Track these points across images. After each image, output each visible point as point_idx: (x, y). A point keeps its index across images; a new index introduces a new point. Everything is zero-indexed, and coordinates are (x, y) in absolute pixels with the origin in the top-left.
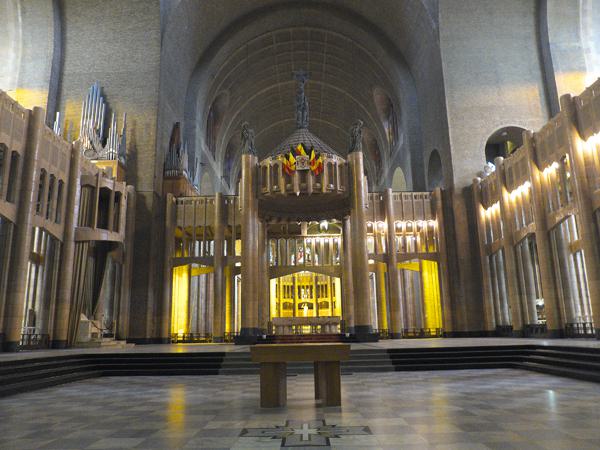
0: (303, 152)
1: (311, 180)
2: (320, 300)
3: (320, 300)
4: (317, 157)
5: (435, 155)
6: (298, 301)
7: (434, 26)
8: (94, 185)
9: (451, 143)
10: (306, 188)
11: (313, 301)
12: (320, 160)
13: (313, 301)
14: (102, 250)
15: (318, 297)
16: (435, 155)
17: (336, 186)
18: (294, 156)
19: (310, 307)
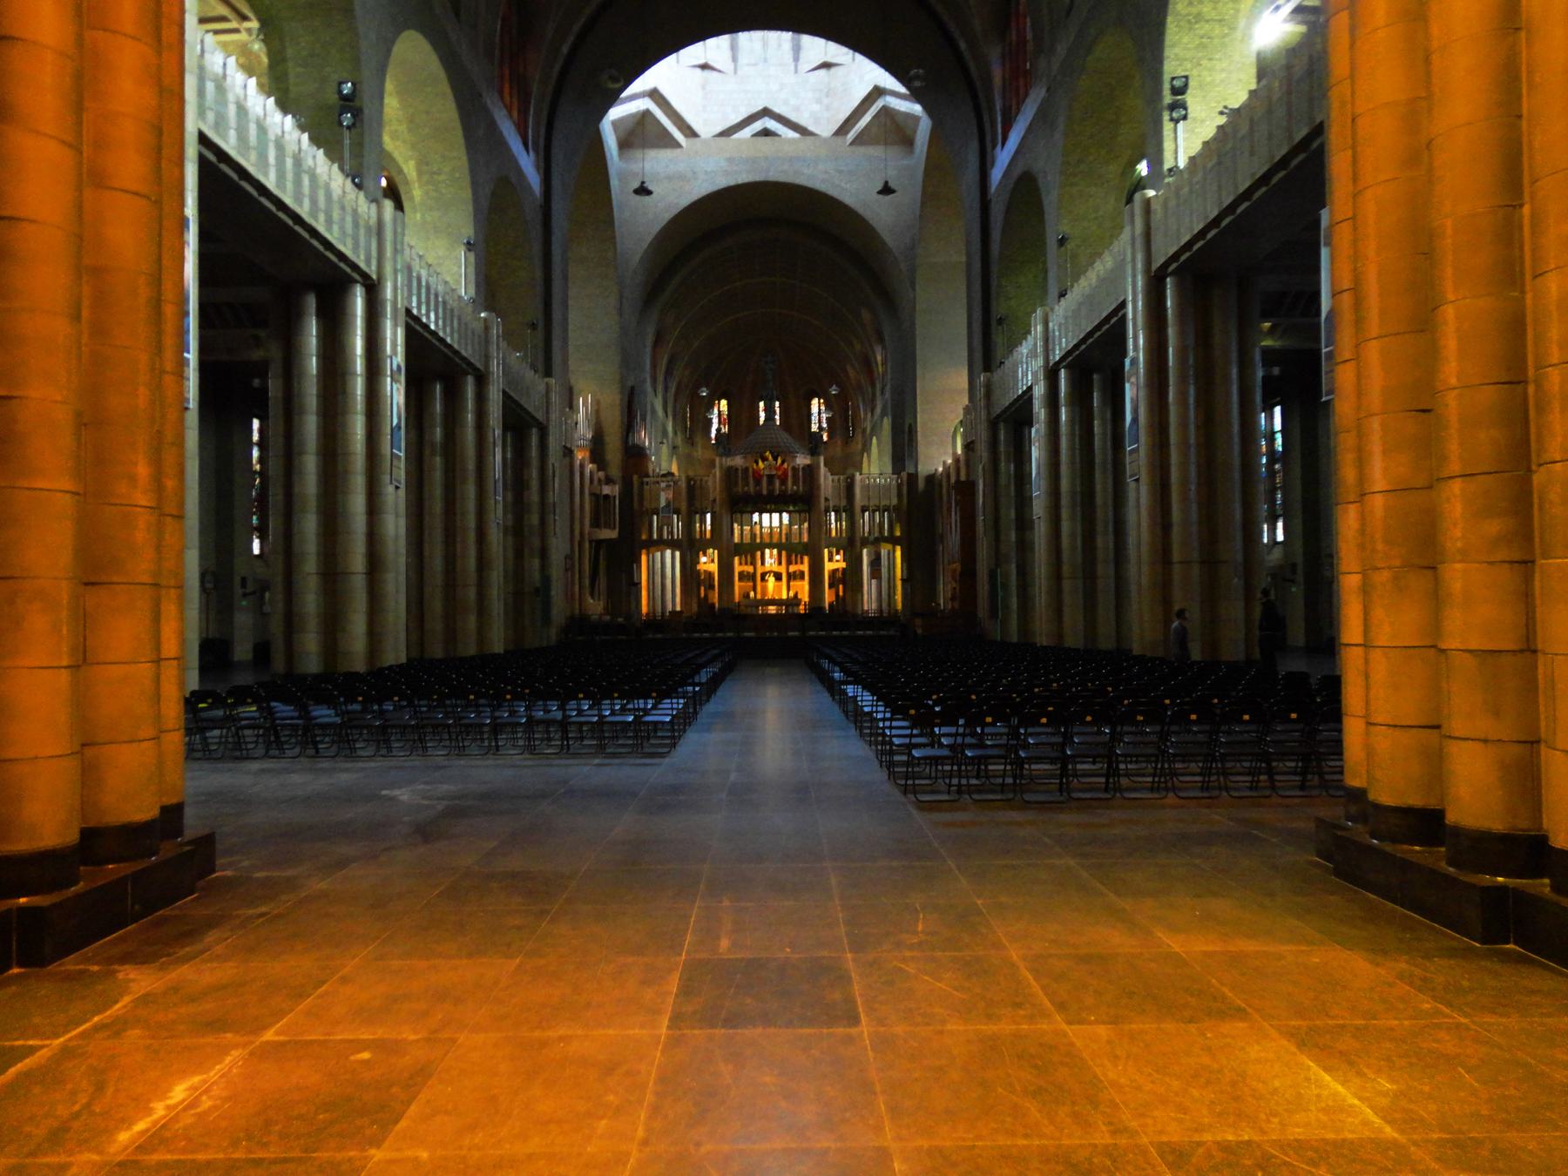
0: (770, 458)
1: (777, 483)
2: (792, 568)
3: (792, 568)
4: (783, 462)
5: (910, 425)
6: (759, 571)
7: (912, 296)
8: (598, 492)
9: (919, 429)
10: (773, 490)
11: (782, 569)
12: (785, 465)
13: (782, 569)
14: (598, 544)
15: (789, 563)
16: (910, 425)
17: (798, 487)
18: (763, 461)
19: (778, 577)
